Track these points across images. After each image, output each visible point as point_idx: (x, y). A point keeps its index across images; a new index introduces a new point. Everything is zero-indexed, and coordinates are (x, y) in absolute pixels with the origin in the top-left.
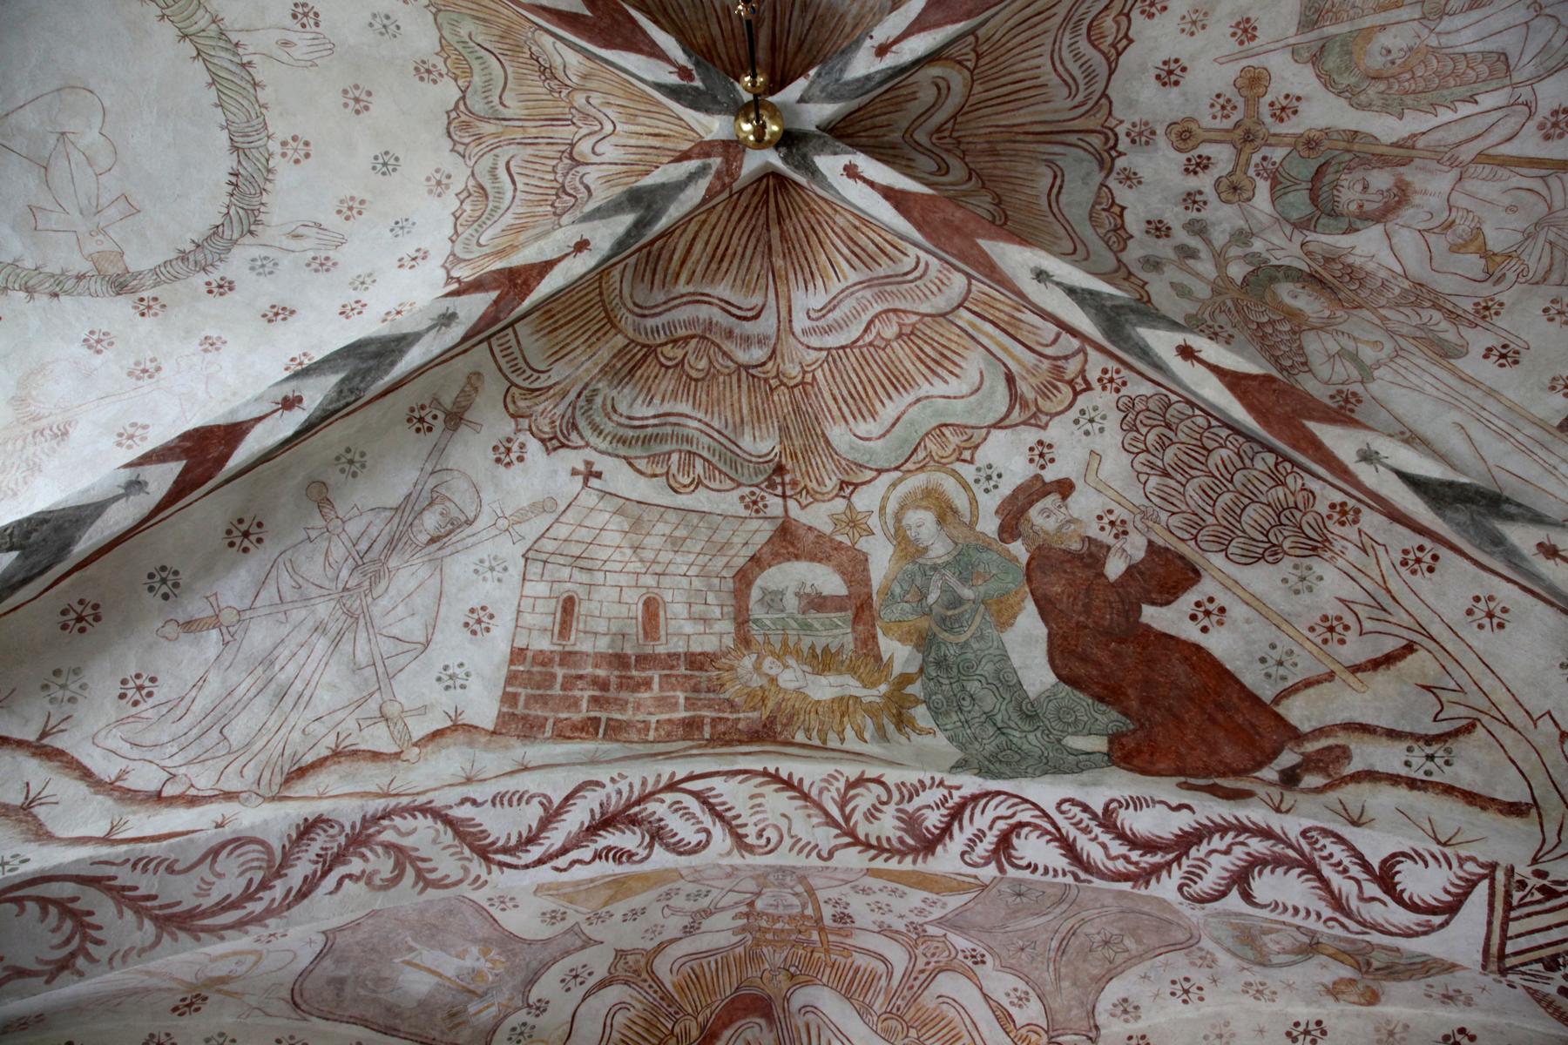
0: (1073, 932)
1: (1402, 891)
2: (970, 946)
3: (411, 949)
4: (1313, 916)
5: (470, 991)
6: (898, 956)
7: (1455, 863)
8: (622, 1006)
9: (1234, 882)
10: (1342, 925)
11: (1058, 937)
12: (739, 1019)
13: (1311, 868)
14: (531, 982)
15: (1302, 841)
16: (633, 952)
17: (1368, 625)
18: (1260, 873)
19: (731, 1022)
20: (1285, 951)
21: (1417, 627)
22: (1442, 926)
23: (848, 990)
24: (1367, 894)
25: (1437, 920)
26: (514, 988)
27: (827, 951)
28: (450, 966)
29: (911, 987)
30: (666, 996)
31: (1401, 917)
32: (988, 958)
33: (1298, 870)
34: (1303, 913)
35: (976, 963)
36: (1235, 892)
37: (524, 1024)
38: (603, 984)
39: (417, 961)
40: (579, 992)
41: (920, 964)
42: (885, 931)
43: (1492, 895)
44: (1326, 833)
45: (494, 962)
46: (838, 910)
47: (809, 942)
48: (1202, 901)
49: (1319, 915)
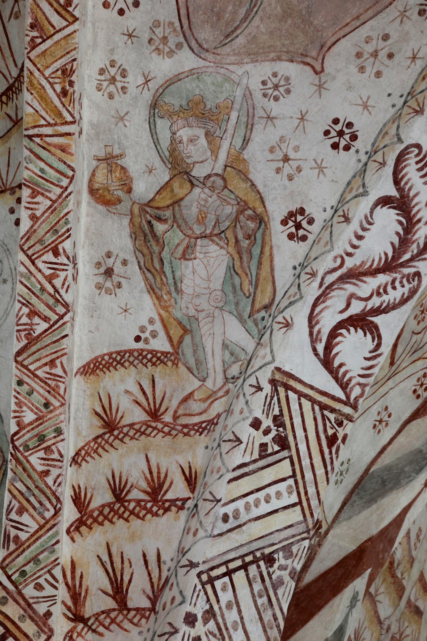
1: (348, 331)
4: (350, 250)
7: (363, 381)
9: (402, 197)
10: (334, 270)
13: (388, 266)
15: (412, 270)
17: (415, 337)
18: (400, 223)
20: (174, 142)
21: (397, 371)
22: (315, 350)
24: (354, 302)
25: (321, 348)
31: (328, 320)
33: (390, 255)
34: (355, 242)
36: (393, 192)
43: (333, 398)
44: (413, 292)
48: (400, 159)
49: (349, 255)
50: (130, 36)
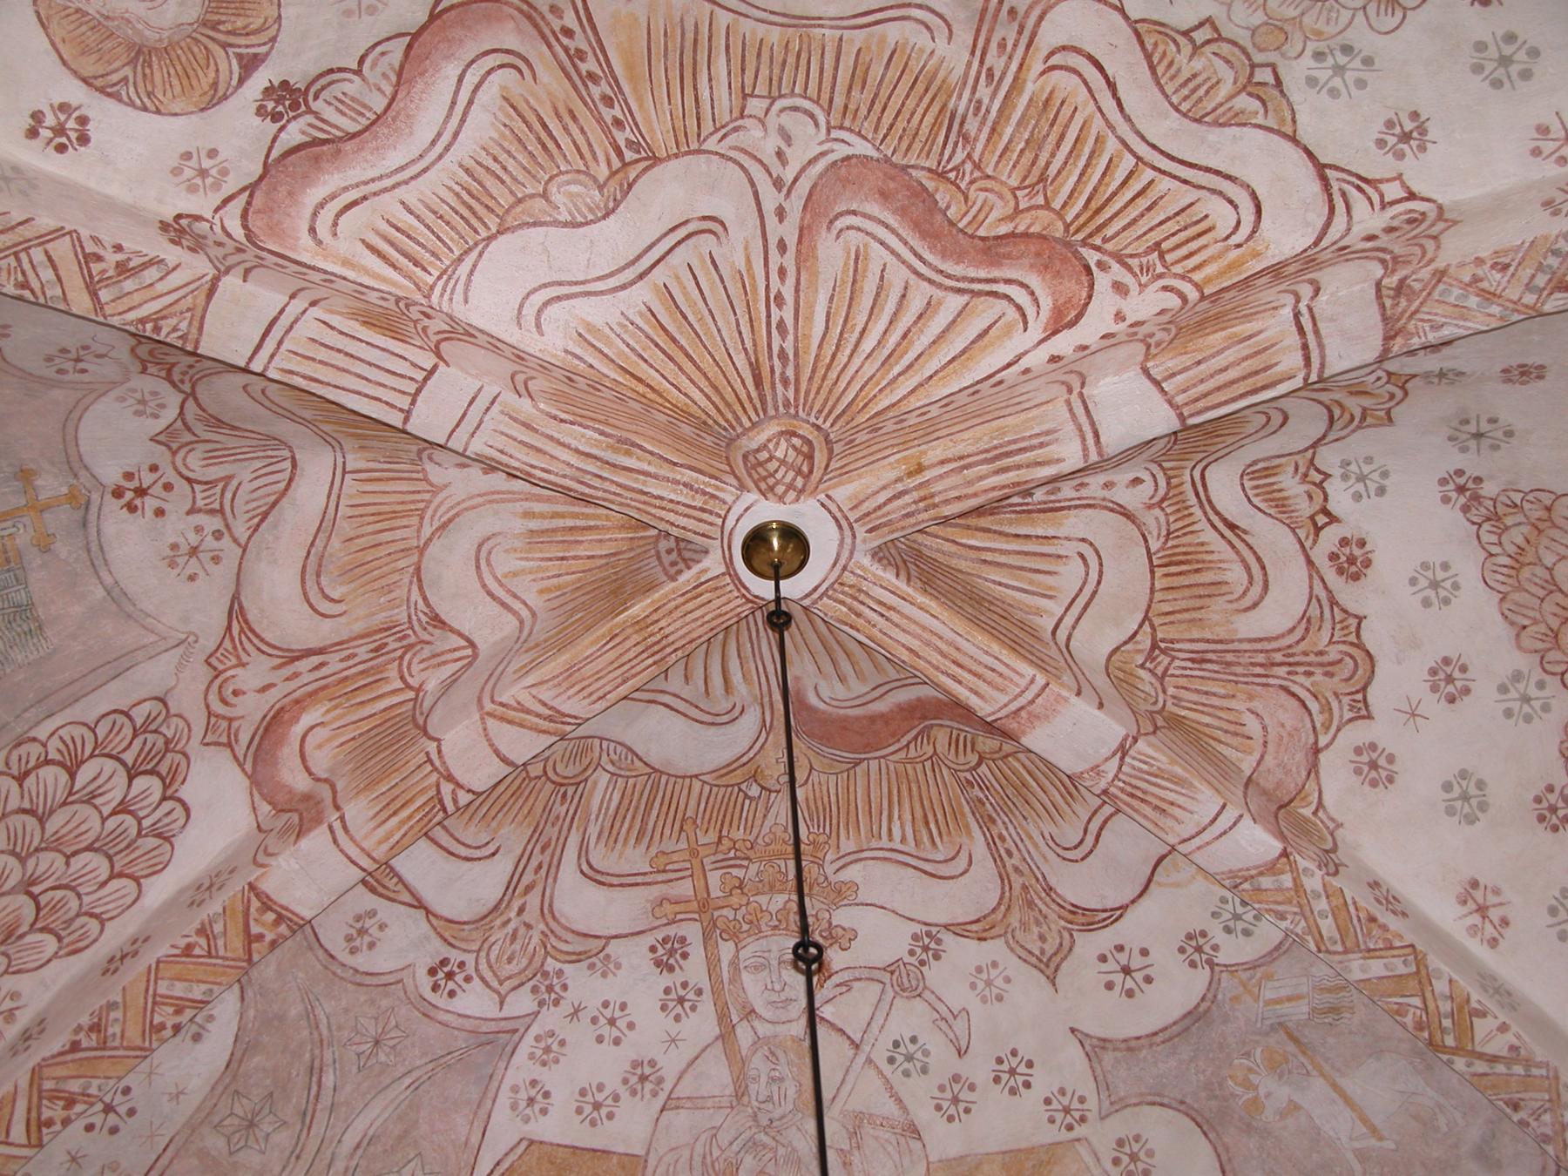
0: (306, 1118)
2: (458, 1004)
3: (1362, 1156)
5: (1295, 1040)
6: (580, 904)
8: (1064, 852)
11: (326, 1100)
12: (857, 719)
14: (1196, 1017)
16: (1027, 956)
19: (872, 719)
23: (655, 787)
26: (1226, 1020)
27: (694, 853)
28: (1315, 1097)
29: (543, 850)
30: (987, 822)
32: (425, 983)
35: (445, 962)
37: (1228, 930)
38: (1089, 919)
39: (1364, 1130)
40: (1128, 930)
41: (533, 900)
42: (594, 950)
45: (1248, 1085)
46: (678, 977)
47: (723, 864)
50: (74, 1159)
